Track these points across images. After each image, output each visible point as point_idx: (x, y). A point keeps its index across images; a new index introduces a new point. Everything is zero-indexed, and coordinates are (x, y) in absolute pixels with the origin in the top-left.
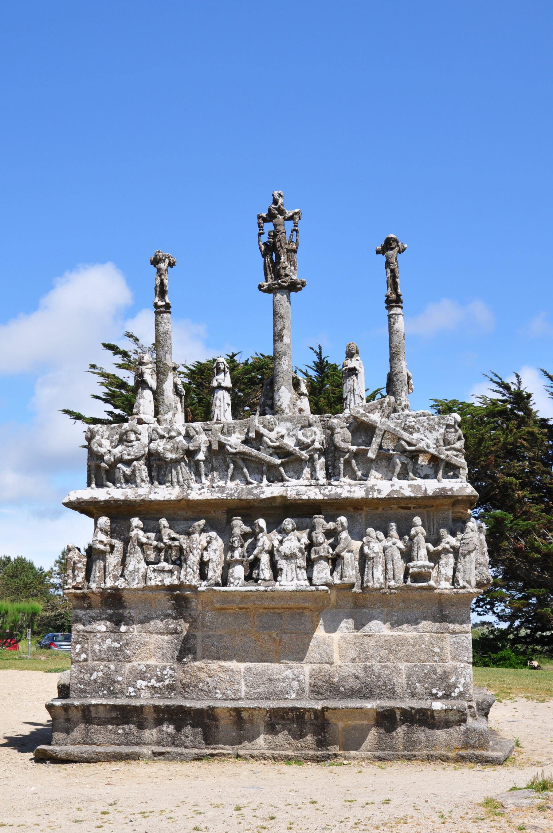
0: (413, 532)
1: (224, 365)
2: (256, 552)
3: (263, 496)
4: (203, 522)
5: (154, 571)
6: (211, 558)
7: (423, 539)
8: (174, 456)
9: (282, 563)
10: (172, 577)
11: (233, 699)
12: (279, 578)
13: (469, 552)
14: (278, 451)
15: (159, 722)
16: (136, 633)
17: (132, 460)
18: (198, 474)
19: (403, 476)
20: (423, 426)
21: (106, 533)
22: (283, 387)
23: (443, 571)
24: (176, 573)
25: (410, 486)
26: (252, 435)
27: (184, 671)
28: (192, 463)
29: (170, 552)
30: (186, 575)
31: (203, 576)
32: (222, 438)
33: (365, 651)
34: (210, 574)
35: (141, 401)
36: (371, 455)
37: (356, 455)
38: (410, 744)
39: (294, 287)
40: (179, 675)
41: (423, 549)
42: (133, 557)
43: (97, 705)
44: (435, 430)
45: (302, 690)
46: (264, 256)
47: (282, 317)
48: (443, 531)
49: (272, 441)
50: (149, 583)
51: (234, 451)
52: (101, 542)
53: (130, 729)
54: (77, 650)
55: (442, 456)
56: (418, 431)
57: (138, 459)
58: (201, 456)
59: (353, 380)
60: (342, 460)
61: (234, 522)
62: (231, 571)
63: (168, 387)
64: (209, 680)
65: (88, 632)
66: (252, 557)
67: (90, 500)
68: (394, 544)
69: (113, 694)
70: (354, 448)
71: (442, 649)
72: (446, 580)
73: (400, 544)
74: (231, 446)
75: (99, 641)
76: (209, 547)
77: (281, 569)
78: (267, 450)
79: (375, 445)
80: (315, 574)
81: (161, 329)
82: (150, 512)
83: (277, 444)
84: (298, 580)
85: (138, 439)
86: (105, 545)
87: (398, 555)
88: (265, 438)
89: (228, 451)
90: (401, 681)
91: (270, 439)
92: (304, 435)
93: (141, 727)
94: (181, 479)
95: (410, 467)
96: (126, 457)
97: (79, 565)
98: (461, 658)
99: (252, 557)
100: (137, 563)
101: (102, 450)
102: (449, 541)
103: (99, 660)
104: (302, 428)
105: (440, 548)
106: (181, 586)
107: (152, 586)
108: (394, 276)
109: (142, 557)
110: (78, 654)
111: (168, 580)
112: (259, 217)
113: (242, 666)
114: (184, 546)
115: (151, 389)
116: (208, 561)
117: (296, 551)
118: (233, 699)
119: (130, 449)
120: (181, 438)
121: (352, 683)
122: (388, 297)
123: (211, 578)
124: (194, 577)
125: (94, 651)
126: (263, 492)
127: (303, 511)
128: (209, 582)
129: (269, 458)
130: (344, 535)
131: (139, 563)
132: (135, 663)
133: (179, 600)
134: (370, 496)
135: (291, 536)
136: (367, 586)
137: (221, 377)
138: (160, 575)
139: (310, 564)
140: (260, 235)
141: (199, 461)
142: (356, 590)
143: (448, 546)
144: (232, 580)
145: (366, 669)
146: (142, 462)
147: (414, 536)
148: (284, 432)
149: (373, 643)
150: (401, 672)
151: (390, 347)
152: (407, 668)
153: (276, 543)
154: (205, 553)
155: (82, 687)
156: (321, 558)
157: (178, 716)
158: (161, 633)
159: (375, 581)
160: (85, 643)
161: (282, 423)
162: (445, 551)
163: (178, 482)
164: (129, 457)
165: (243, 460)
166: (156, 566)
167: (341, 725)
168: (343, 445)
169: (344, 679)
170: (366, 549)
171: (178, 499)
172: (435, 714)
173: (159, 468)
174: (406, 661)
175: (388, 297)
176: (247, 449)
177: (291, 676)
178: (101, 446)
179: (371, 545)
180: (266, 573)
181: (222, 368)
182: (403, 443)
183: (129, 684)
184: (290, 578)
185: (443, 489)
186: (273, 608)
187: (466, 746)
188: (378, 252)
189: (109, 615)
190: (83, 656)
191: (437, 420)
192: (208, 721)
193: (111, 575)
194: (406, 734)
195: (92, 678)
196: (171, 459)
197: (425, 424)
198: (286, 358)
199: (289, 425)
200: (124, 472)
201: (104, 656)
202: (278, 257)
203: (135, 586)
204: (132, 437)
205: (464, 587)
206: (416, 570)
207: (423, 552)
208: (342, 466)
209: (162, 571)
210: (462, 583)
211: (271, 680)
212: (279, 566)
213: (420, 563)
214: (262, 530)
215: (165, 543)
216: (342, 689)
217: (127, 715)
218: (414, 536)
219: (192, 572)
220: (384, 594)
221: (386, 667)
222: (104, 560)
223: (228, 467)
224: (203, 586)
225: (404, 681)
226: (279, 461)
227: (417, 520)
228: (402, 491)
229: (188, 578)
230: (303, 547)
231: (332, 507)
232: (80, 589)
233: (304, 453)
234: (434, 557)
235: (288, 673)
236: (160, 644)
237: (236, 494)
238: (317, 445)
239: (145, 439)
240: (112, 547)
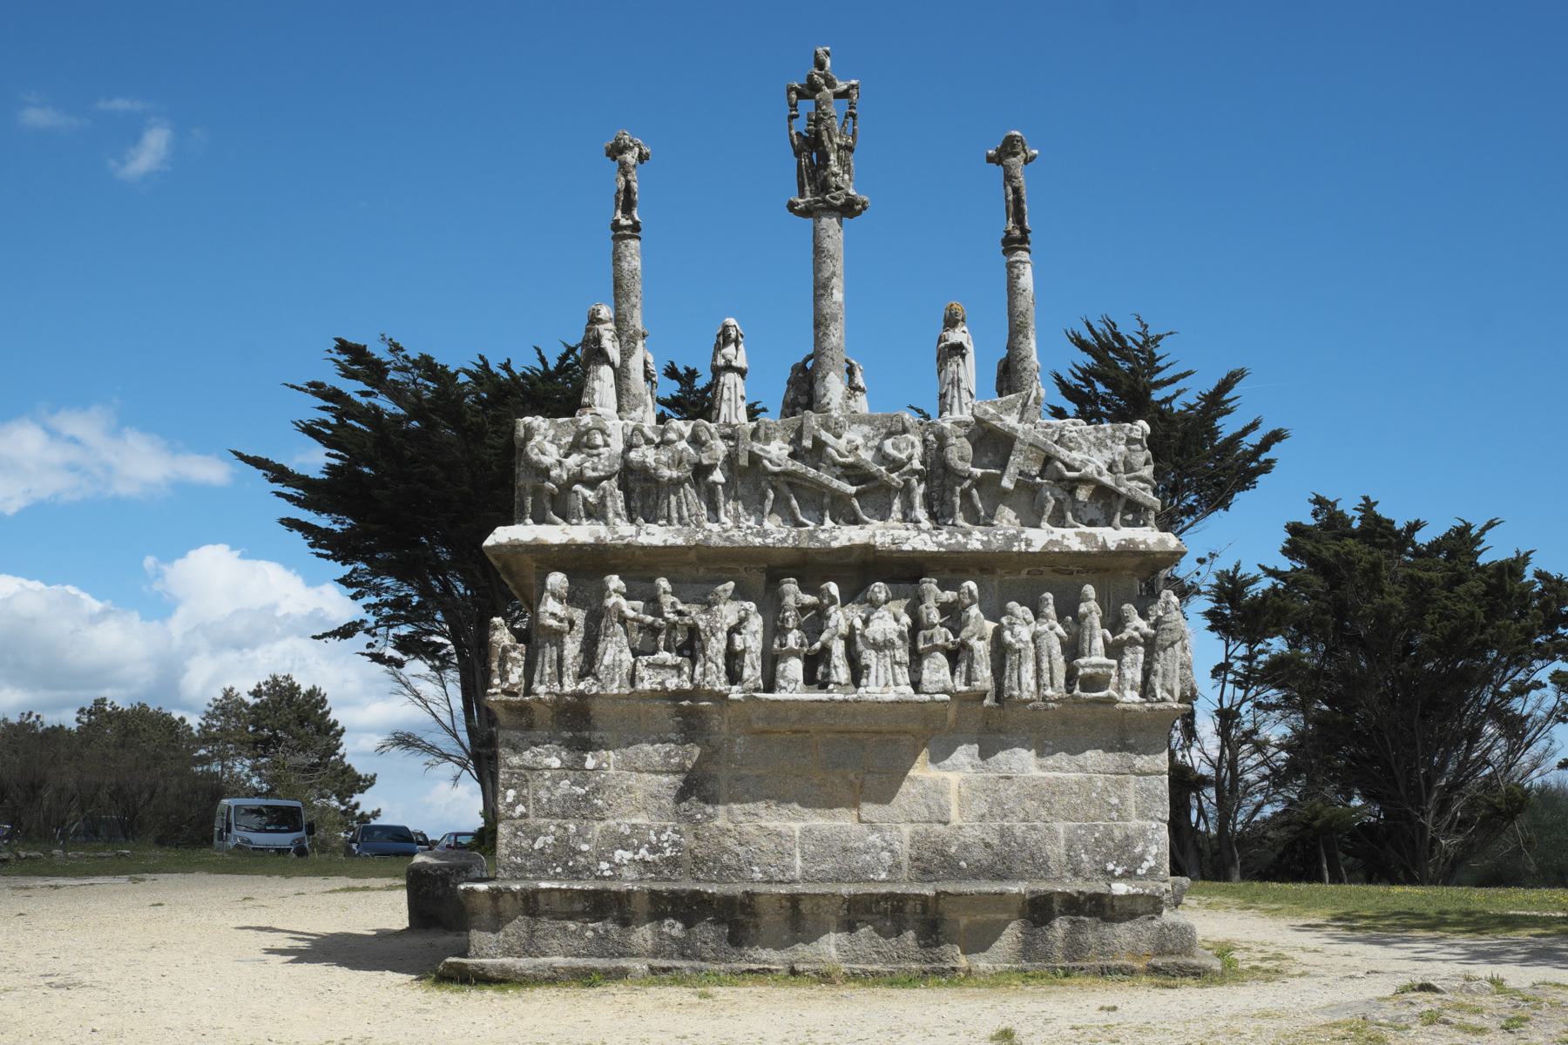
0: (1083, 608)
2: (824, 636)
3: (835, 544)
4: (731, 584)
5: (649, 665)
7: (1097, 623)
8: (675, 474)
9: (869, 657)
11: (781, 882)
12: (864, 681)
13: (1173, 644)
14: (850, 473)
15: (657, 916)
16: (612, 771)
17: (601, 479)
18: (713, 509)
19: (1058, 520)
20: (1086, 440)
22: (832, 374)
23: (1128, 675)
24: (686, 669)
25: (1077, 534)
26: (808, 443)
27: (696, 836)
28: (703, 488)
30: (704, 674)
31: (734, 677)
32: (757, 447)
33: (1001, 804)
34: (747, 672)
35: (597, 384)
36: (1007, 483)
37: (978, 483)
38: (1075, 950)
39: (849, 209)
40: (687, 840)
41: (1098, 637)
43: (552, 890)
44: (1106, 446)
45: (898, 866)
46: (798, 154)
47: (832, 257)
48: (1129, 609)
49: (841, 455)
50: (639, 687)
51: (776, 469)
52: (553, 615)
53: (607, 931)
54: (509, 800)
55: (1123, 490)
56: (1080, 448)
57: (608, 478)
58: (718, 476)
60: (958, 489)
61: (786, 587)
62: (781, 667)
63: (636, 364)
64: (738, 849)
65: (527, 768)
66: (817, 645)
68: (1052, 628)
69: (575, 874)
70: (978, 472)
71: (1123, 800)
72: (1132, 688)
73: (1059, 629)
75: (548, 783)
77: (868, 667)
79: (1012, 470)
80: (926, 675)
81: (625, 265)
82: (640, 567)
83: (851, 459)
84: (897, 684)
85: (607, 445)
86: (561, 620)
87: (1057, 649)
88: (830, 450)
89: (765, 468)
90: (1056, 851)
92: (896, 447)
93: (625, 922)
94: (686, 514)
95: (1068, 504)
96: (589, 473)
97: (514, 654)
98: (1152, 814)
99: (817, 645)
100: (615, 651)
101: (547, 460)
102: (1138, 625)
103: (548, 815)
104: (890, 434)
105: (1124, 636)
106: (696, 693)
107: (645, 691)
108: (1018, 201)
109: (625, 641)
110: (512, 806)
111: (672, 683)
112: (790, 89)
113: (797, 827)
114: (702, 625)
115: (612, 365)
116: (744, 651)
117: (894, 637)
118: (781, 882)
119: (596, 459)
120: (683, 444)
121: (978, 854)
122: (1008, 233)
125: (539, 800)
126: (836, 538)
127: (905, 572)
129: (836, 483)
130: (974, 611)
132: (612, 822)
133: (688, 715)
134: (1015, 549)
135: (882, 611)
136: (1011, 696)
137: (730, 350)
139: (916, 659)
140: (792, 117)
141: (715, 484)
142: (987, 702)
143: (1136, 634)
144: (782, 682)
145: (1003, 833)
146: (614, 482)
147: (1085, 616)
148: (860, 441)
149: (1012, 790)
150: (1057, 835)
151: (1011, 315)
152: (1068, 830)
153: (858, 624)
154: (738, 638)
155: (519, 860)
156: (936, 648)
157: (689, 908)
158: (656, 772)
159: (1024, 687)
160: (523, 787)
162: (1132, 642)
163: (681, 519)
164: (595, 474)
165: (790, 485)
166: (651, 659)
167: (964, 921)
168: (960, 465)
169: (965, 847)
170: (1007, 635)
172: (1116, 902)
173: (645, 494)
174: (1066, 819)
175: (1008, 233)
176: (797, 466)
177: (879, 843)
178: (543, 453)
179: (1017, 629)
180: (842, 673)
182: (1060, 465)
183: (601, 856)
184: (882, 682)
185: (1131, 541)
186: (849, 732)
187: (1161, 951)
188: (990, 159)
189: (565, 740)
190: (520, 809)
191: (1109, 431)
192: (742, 917)
194: (1069, 934)
195: (536, 847)
196: (670, 479)
197: (1091, 438)
199: (866, 429)
200: (585, 499)
201: (557, 810)
202: (824, 157)
204: (599, 440)
205: (1163, 700)
206: (1088, 670)
207: (1098, 643)
208: (958, 501)
209: (663, 666)
210: (1159, 693)
211: (845, 850)
212: (863, 662)
213: (1095, 660)
214: (833, 601)
215: (666, 619)
216: (963, 864)
217: (606, 906)
218: (1085, 616)
220: (1035, 709)
221: (1034, 828)
222: (560, 646)
223: (764, 496)
224: (736, 693)
225: (1063, 851)
227: (1089, 590)
228: (1066, 542)
230: (906, 629)
231: (951, 567)
232: (516, 695)
233: (894, 475)
234: (1114, 650)
235: (874, 838)
236: (654, 790)
237: (790, 541)
238: (917, 464)
239: (618, 446)
240: (572, 623)
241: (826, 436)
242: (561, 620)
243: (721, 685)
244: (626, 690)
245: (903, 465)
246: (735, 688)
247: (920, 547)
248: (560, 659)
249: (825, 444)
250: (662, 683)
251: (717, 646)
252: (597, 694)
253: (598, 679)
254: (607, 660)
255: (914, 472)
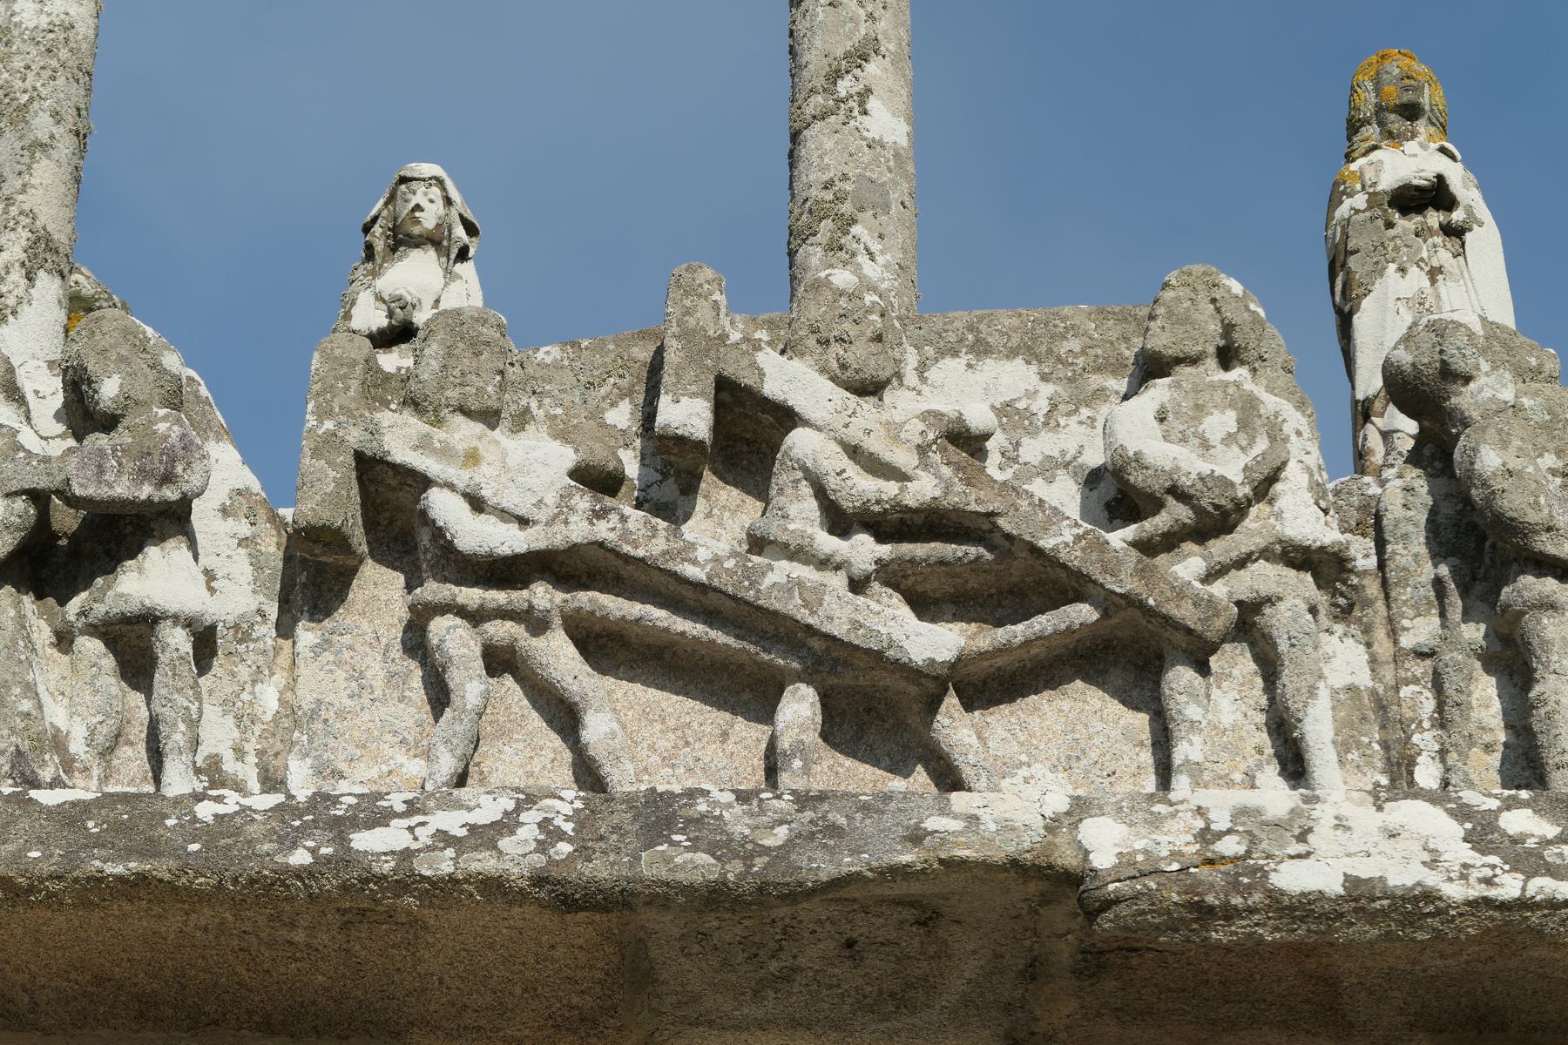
1: (448, 202)
26: (687, 414)
51: (507, 540)
59: (1434, 273)
74: (477, 504)
78: (826, 543)
83: (923, 489)
91: (854, 451)
137: (414, 276)
148: (978, 417)
161: (948, 363)
181: (429, 219)
198: (888, 222)
226: (935, 642)
241: (786, 378)
245: (1215, 521)
247: (1403, 874)
249: (787, 418)
255: (1299, 557)
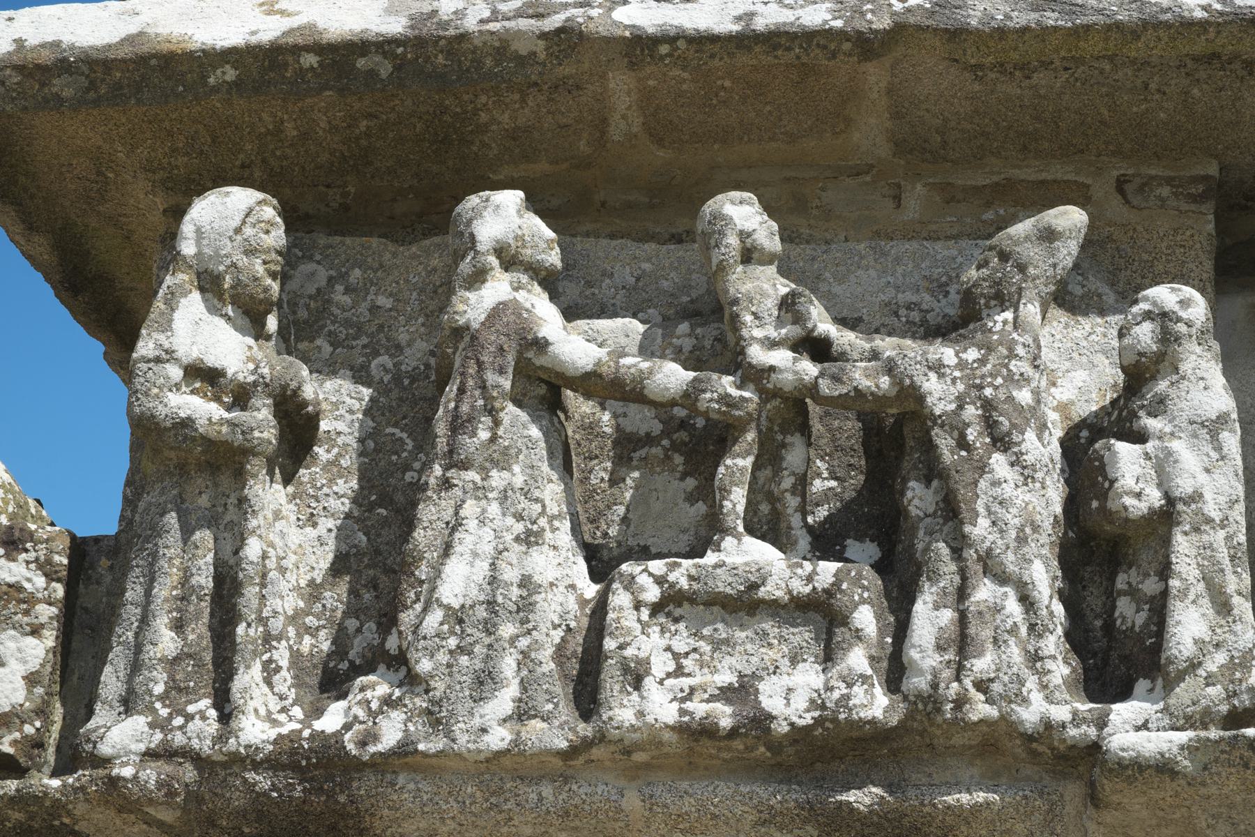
4: (1071, 218)
5: (671, 604)
6: (1184, 486)
10: (828, 658)
21: (250, 315)
24: (865, 618)
29: (794, 457)
30: (961, 643)
31: (1117, 657)
42: (480, 492)
50: (622, 712)
52: (204, 376)
67: (126, 52)
76: (1159, 407)
100: (506, 540)
106: (921, 738)
109: (552, 492)
111: (792, 692)
114: (939, 393)
116: (1165, 517)
123: (1194, 665)
124: (1034, 659)
128: (1183, 693)
131: (530, 539)
138: (717, 645)
154: (1128, 461)
171: (860, 25)
193: (282, 655)
203: (498, 738)
209: (745, 604)
215: (756, 376)
219: (1013, 607)
222: (230, 522)
224: (1135, 728)
229: (982, 664)
240: (299, 430)
242: (241, 397)
243: (1049, 700)
244: (553, 732)
246: (1123, 712)
248: (228, 583)
250: (741, 691)
251: (1019, 501)
252: (404, 750)
253: (412, 681)
254: (459, 581)
